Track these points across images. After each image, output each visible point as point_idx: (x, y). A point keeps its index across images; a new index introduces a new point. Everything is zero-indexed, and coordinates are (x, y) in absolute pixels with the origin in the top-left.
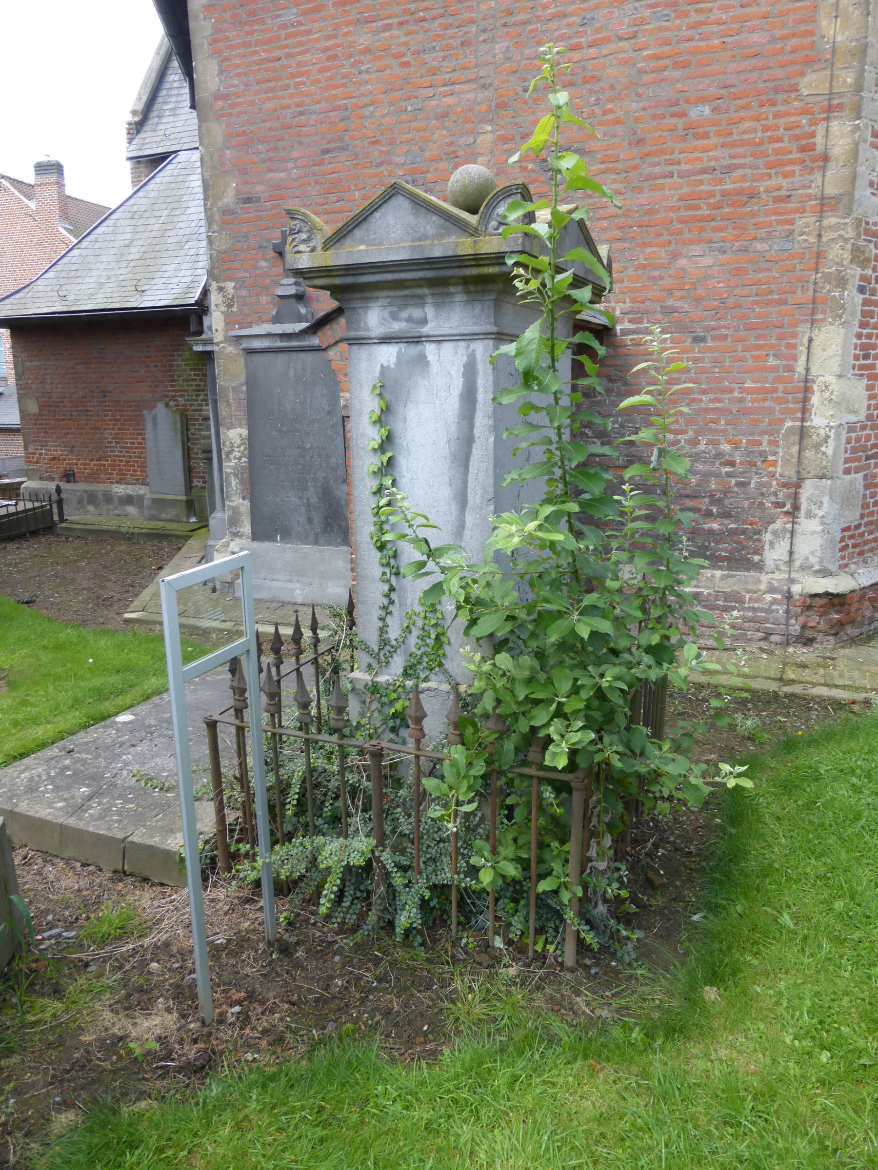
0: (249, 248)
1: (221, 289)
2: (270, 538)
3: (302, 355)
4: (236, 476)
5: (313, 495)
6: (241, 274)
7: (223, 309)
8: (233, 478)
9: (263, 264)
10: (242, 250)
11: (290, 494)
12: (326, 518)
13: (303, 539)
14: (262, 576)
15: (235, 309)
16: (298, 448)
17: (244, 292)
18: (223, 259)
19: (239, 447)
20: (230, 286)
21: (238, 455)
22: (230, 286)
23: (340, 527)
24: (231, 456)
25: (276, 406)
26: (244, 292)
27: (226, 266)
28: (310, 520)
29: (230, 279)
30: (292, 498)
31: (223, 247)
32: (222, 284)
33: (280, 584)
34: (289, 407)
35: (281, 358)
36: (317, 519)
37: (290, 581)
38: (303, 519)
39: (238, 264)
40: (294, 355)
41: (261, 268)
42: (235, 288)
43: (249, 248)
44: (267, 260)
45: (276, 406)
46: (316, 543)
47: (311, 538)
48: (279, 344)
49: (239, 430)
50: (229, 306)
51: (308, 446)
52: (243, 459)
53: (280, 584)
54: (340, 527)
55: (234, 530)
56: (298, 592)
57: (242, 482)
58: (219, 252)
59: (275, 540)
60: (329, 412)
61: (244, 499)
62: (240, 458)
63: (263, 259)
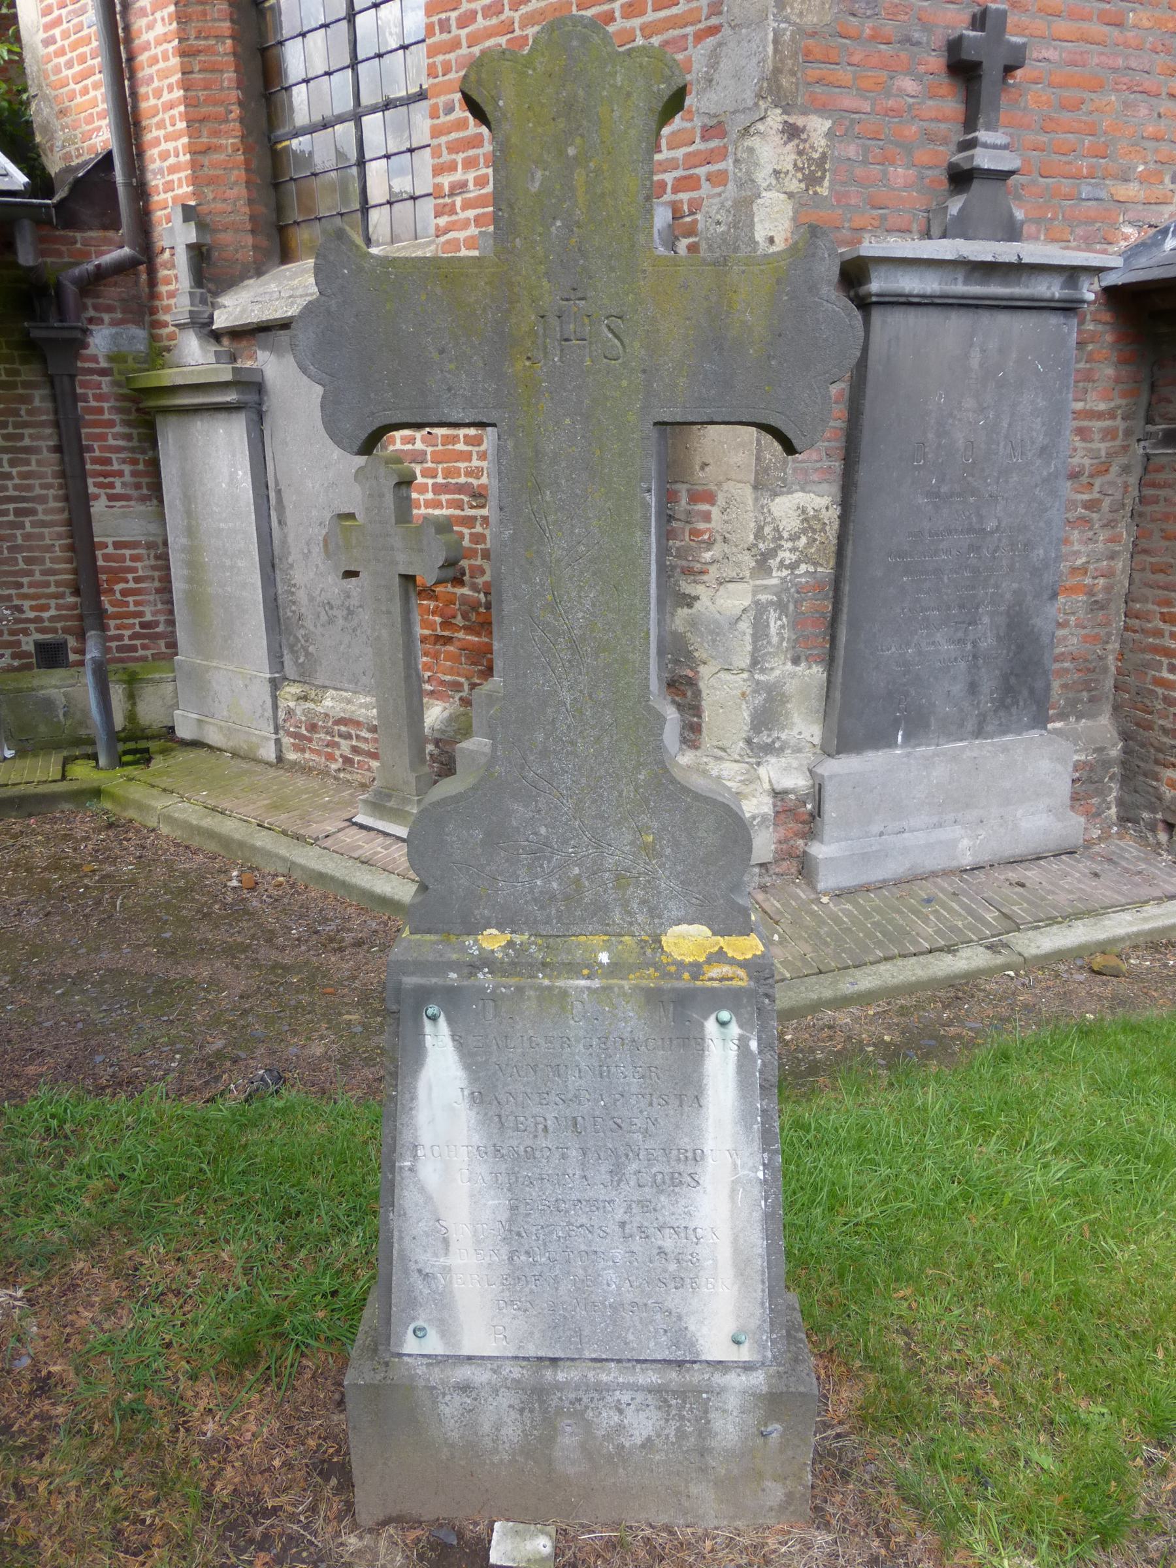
0: (875, 38)
1: (792, 132)
2: (879, 739)
3: (1003, 318)
4: (781, 606)
5: (986, 634)
6: (849, 102)
7: (794, 185)
8: (773, 615)
9: (908, 84)
10: (856, 38)
11: (938, 637)
12: (1005, 678)
13: (954, 729)
14: (876, 828)
15: (824, 190)
16: (970, 530)
17: (851, 151)
18: (808, 53)
19: (794, 538)
20: (818, 127)
21: (787, 556)
22: (818, 127)
23: (1032, 691)
24: (773, 563)
25: (930, 436)
26: (851, 151)
27: (814, 72)
28: (973, 688)
29: (822, 110)
30: (943, 645)
31: (811, 19)
32: (800, 121)
33: (921, 838)
34: (960, 438)
35: (956, 323)
36: (988, 683)
37: (940, 825)
38: (958, 689)
39: (844, 74)
40: (986, 319)
41: (902, 93)
42: (829, 134)
43: (875, 38)
44: (918, 78)
45: (930, 436)
46: (979, 733)
47: (970, 725)
48: (960, 287)
49: (799, 498)
50: (812, 180)
51: (991, 525)
52: (803, 568)
53: (921, 838)
54: (1032, 691)
55: (765, 738)
56: (965, 843)
57: (794, 625)
58: (800, 30)
59: (892, 744)
60: (1043, 450)
61: (796, 661)
62: (793, 566)
63: (909, 72)
